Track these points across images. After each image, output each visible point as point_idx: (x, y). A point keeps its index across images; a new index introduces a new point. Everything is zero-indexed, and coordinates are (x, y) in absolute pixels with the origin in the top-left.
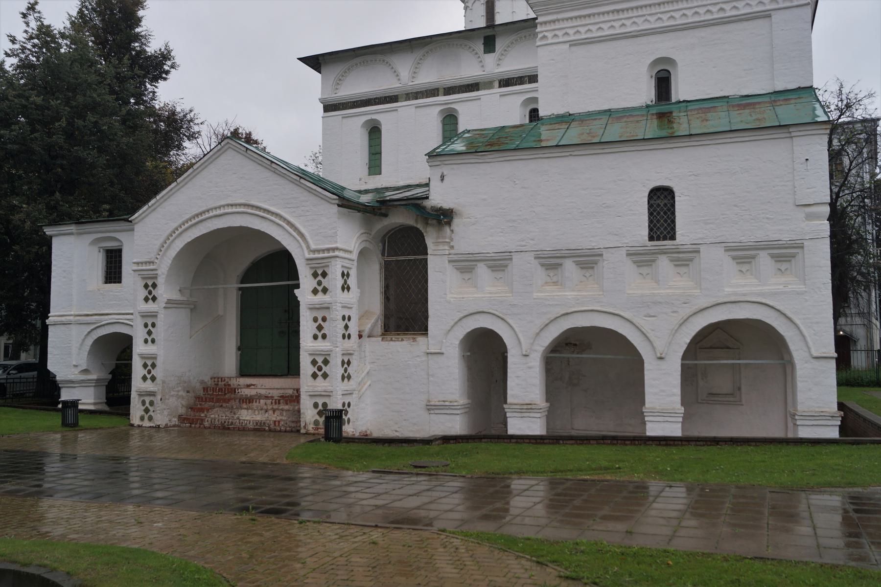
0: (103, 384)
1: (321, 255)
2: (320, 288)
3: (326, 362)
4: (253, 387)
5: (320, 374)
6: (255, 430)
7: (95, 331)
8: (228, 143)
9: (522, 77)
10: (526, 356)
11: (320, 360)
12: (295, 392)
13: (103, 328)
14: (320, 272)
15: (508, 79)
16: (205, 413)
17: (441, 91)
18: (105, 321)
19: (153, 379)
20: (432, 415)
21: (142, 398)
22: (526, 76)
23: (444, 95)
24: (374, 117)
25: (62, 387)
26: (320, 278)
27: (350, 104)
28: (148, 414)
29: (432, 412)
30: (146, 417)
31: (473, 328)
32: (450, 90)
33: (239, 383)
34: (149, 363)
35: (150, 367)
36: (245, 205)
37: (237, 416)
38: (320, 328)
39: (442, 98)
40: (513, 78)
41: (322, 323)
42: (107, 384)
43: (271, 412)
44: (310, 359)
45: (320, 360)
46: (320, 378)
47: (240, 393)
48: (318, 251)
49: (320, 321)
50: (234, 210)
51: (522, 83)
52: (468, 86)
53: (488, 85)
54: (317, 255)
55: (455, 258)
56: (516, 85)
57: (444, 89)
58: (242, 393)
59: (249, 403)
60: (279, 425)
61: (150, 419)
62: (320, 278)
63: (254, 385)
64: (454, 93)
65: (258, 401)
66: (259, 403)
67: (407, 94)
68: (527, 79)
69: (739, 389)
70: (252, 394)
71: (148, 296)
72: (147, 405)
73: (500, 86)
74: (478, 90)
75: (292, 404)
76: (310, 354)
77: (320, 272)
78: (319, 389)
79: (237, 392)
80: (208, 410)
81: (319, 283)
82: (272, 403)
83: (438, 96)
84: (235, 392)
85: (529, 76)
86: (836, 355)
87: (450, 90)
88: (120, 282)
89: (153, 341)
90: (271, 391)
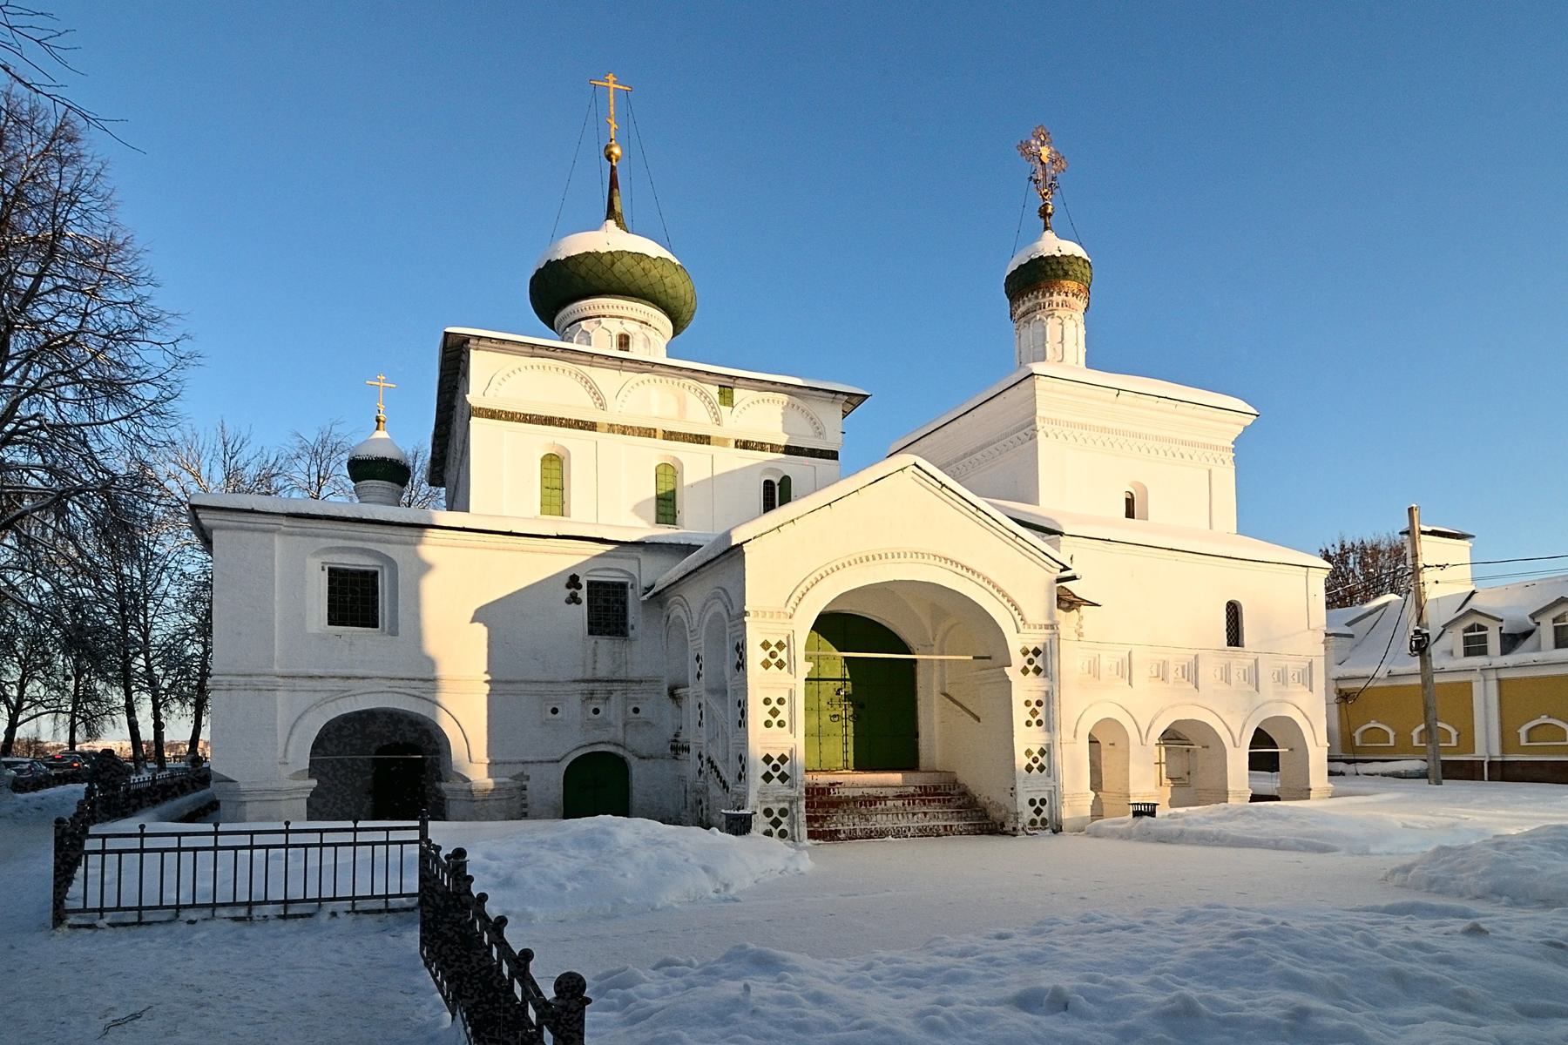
12: (918, 789)
15: (747, 441)
16: (821, 822)
17: (659, 433)
22: (768, 444)
27: (518, 416)
32: (670, 436)
33: (817, 782)
47: (837, 795)
51: (762, 450)
53: (723, 442)
59: (870, 806)
60: (951, 829)
63: (840, 783)
64: (677, 440)
65: (883, 802)
66: (885, 805)
68: (769, 446)
70: (855, 795)
73: (736, 447)
74: (709, 443)
82: (904, 804)
90: (884, 790)
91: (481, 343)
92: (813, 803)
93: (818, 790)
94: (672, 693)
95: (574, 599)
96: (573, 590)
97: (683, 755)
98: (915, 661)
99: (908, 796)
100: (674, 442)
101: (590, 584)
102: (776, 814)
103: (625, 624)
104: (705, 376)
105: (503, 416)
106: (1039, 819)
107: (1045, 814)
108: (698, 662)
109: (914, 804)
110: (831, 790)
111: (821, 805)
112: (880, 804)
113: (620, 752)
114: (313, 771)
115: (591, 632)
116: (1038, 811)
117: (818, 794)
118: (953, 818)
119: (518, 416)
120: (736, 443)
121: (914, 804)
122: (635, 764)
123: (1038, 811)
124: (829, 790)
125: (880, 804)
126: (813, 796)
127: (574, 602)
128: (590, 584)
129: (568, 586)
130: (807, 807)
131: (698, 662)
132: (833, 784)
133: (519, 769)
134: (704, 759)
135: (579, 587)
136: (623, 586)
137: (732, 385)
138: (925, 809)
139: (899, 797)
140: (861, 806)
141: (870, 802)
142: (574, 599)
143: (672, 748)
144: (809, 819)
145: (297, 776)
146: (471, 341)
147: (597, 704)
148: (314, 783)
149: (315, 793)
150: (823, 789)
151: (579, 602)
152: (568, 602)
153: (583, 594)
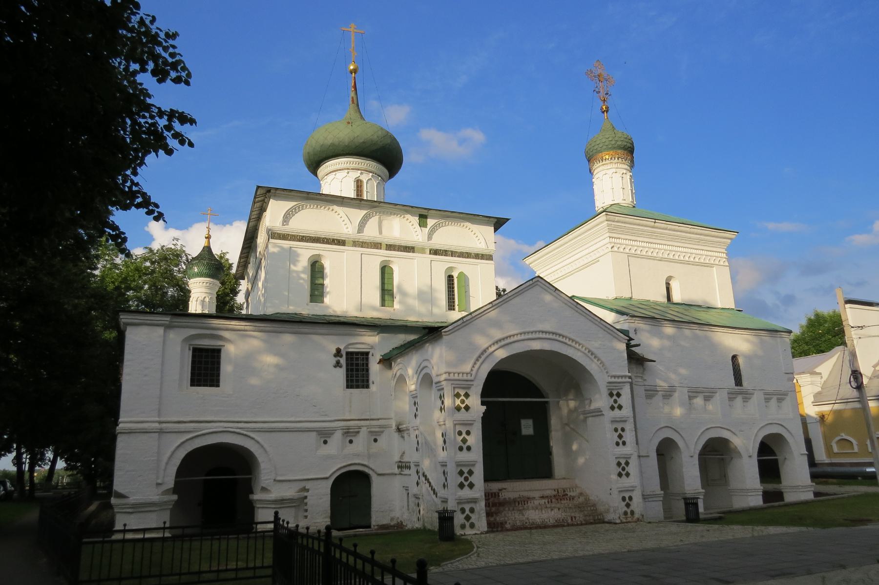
0: (166, 507)
1: (620, 380)
2: (616, 406)
3: (627, 463)
4: (504, 491)
5: (624, 473)
6: (554, 526)
7: (190, 441)
8: (538, 281)
9: (446, 251)
10: (692, 457)
11: (623, 462)
13: (204, 438)
14: (615, 392)
16: (494, 517)
17: (384, 246)
18: (207, 429)
19: (471, 486)
20: (647, 503)
21: (460, 506)
23: (386, 250)
24: (321, 253)
25: (258, 508)
26: (615, 397)
27: (298, 237)
28: (470, 522)
29: (647, 500)
30: (467, 524)
31: (662, 438)
32: (390, 247)
33: (491, 488)
34: (466, 470)
35: (466, 475)
36: (553, 333)
37: (526, 516)
38: (620, 437)
39: (383, 252)
40: (441, 250)
41: (621, 432)
42: (171, 507)
43: (556, 510)
44: (615, 462)
45: (623, 462)
46: (624, 477)
48: (615, 377)
49: (620, 432)
50: (544, 336)
51: (446, 255)
52: (406, 247)
53: (422, 251)
54: (613, 380)
55: (648, 388)
56: (442, 255)
57: (386, 245)
58: (506, 497)
60: (575, 519)
61: (472, 526)
62: (615, 397)
63: (505, 489)
64: (394, 250)
67: (354, 242)
69: (725, 476)
71: (614, 404)
72: (467, 512)
73: (430, 253)
74: (413, 252)
75: (562, 502)
76: (616, 458)
77: (615, 392)
78: (627, 485)
79: (501, 496)
80: (497, 514)
81: (615, 401)
83: (381, 249)
84: (499, 496)
85: (451, 251)
86: (807, 453)
87: (390, 247)
88: (218, 386)
89: (624, 443)
91: (278, 192)
92: (489, 504)
93: (492, 494)
94: (399, 430)
95: (338, 364)
96: (339, 358)
97: (406, 471)
98: (547, 402)
99: (547, 497)
100: (392, 251)
101: (348, 353)
102: (467, 512)
103: (368, 381)
104: (411, 209)
105: (289, 238)
106: (629, 511)
107: (632, 508)
108: (415, 405)
109: (551, 502)
110: (500, 494)
111: (494, 505)
112: (531, 502)
113: (366, 470)
114: (176, 490)
115: (348, 387)
116: (628, 505)
117: (492, 497)
118: (576, 511)
119: (298, 237)
120: (430, 251)
121: (551, 502)
122: (375, 479)
123: (628, 505)
124: (498, 493)
125: (531, 502)
126: (489, 499)
127: (338, 366)
128: (348, 353)
129: (335, 356)
130: (486, 506)
131: (415, 405)
132: (500, 490)
133: (302, 484)
134: (421, 474)
135: (341, 356)
136: (367, 354)
137: (426, 214)
138: (558, 505)
139: (542, 497)
140: (519, 504)
141: (524, 502)
142: (338, 364)
143: (398, 467)
144: (489, 514)
145: (166, 492)
146: (272, 191)
147: (352, 436)
148: (175, 497)
149: (177, 503)
150: (495, 493)
151: (341, 367)
152: (335, 367)
153: (343, 361)
